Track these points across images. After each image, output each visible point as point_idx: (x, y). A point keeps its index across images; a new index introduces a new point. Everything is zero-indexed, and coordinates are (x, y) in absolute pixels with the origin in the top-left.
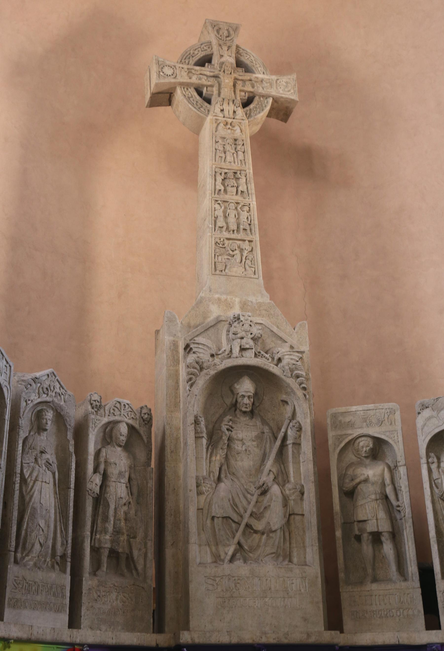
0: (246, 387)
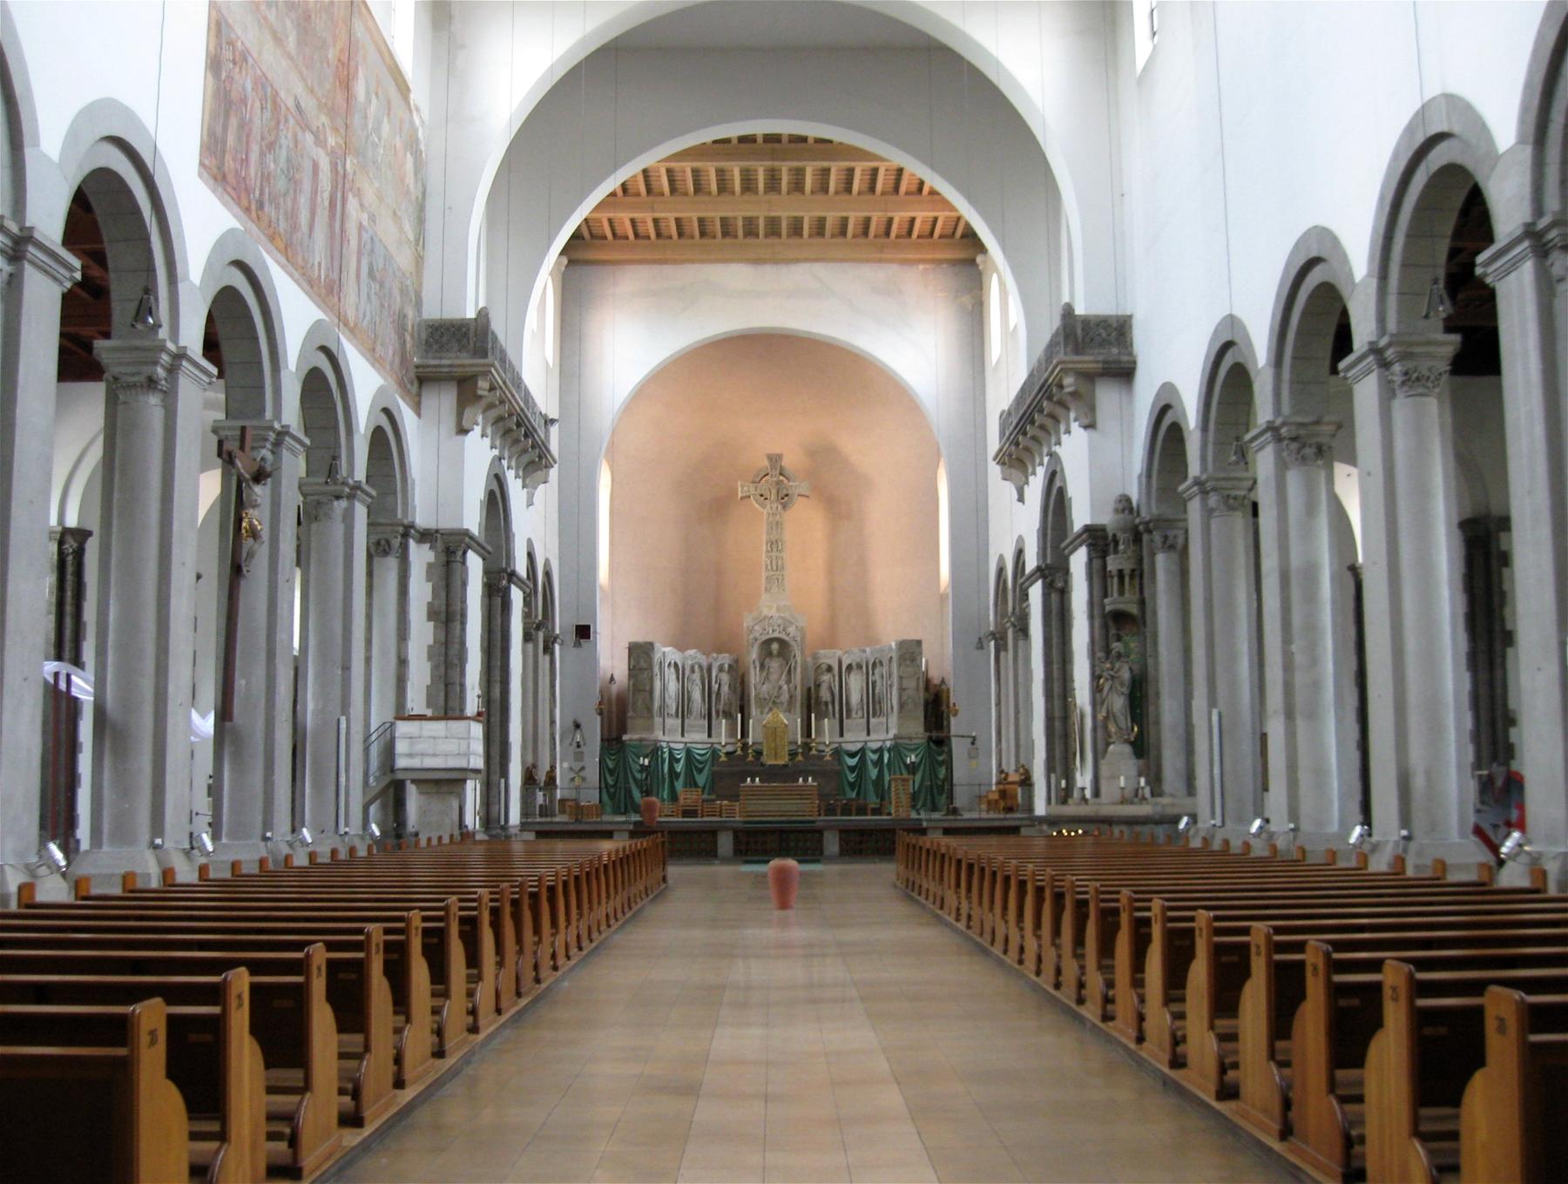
0: (775, 646)
